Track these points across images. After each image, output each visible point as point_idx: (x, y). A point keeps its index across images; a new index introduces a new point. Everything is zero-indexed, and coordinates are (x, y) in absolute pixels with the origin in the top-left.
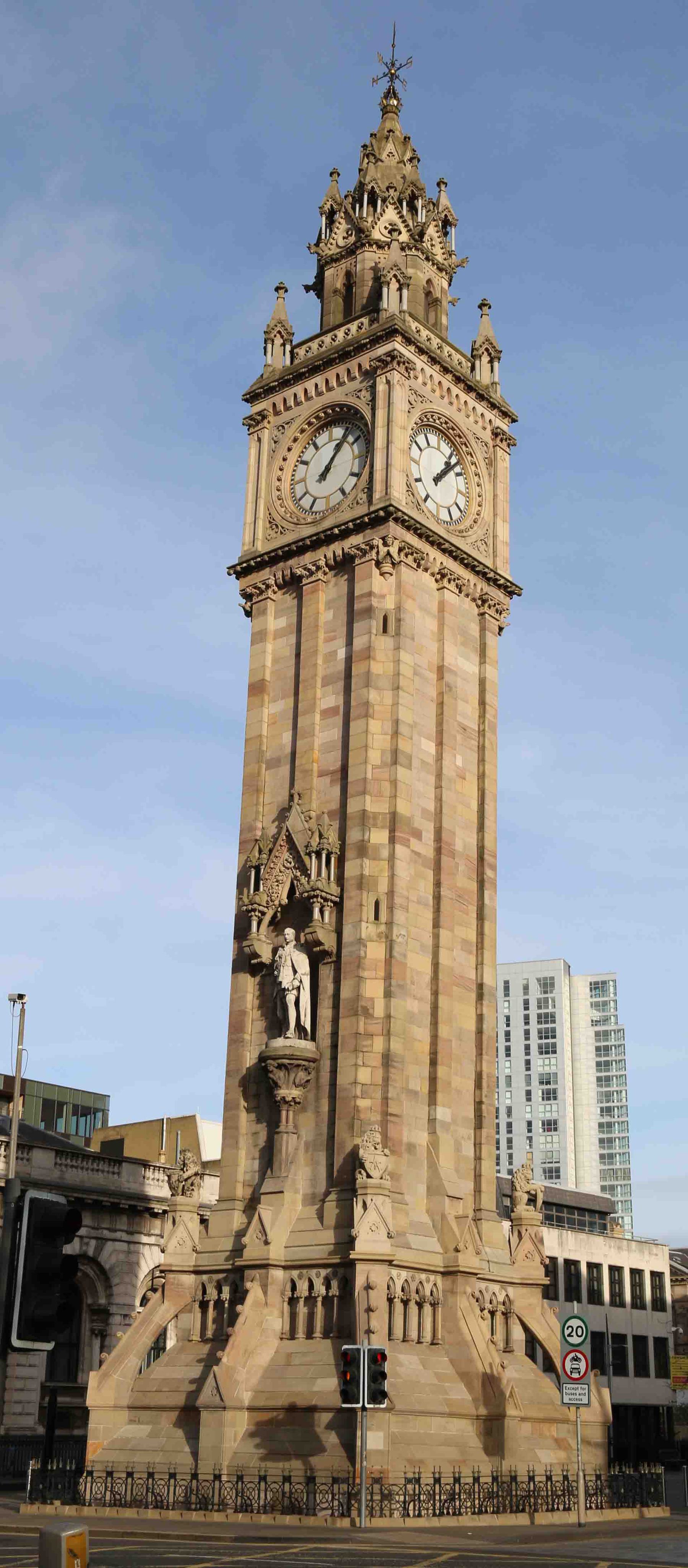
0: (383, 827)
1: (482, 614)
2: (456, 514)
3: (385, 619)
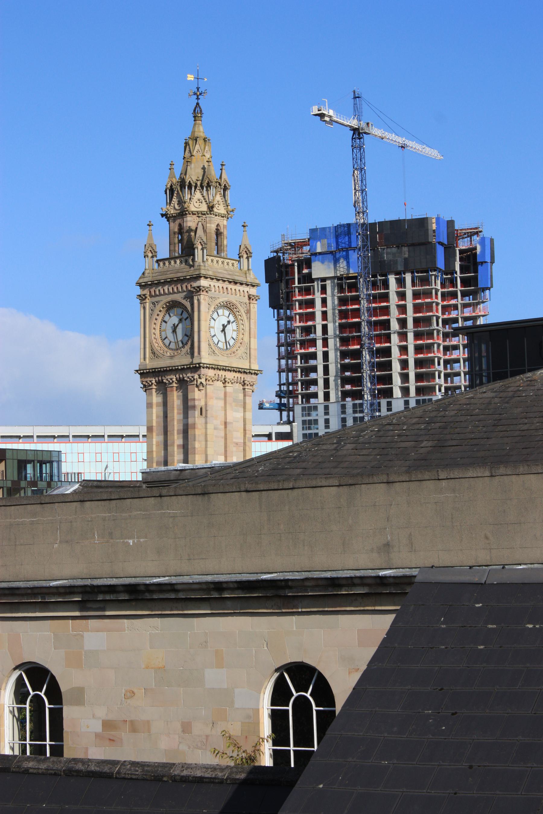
3: (201, 409)
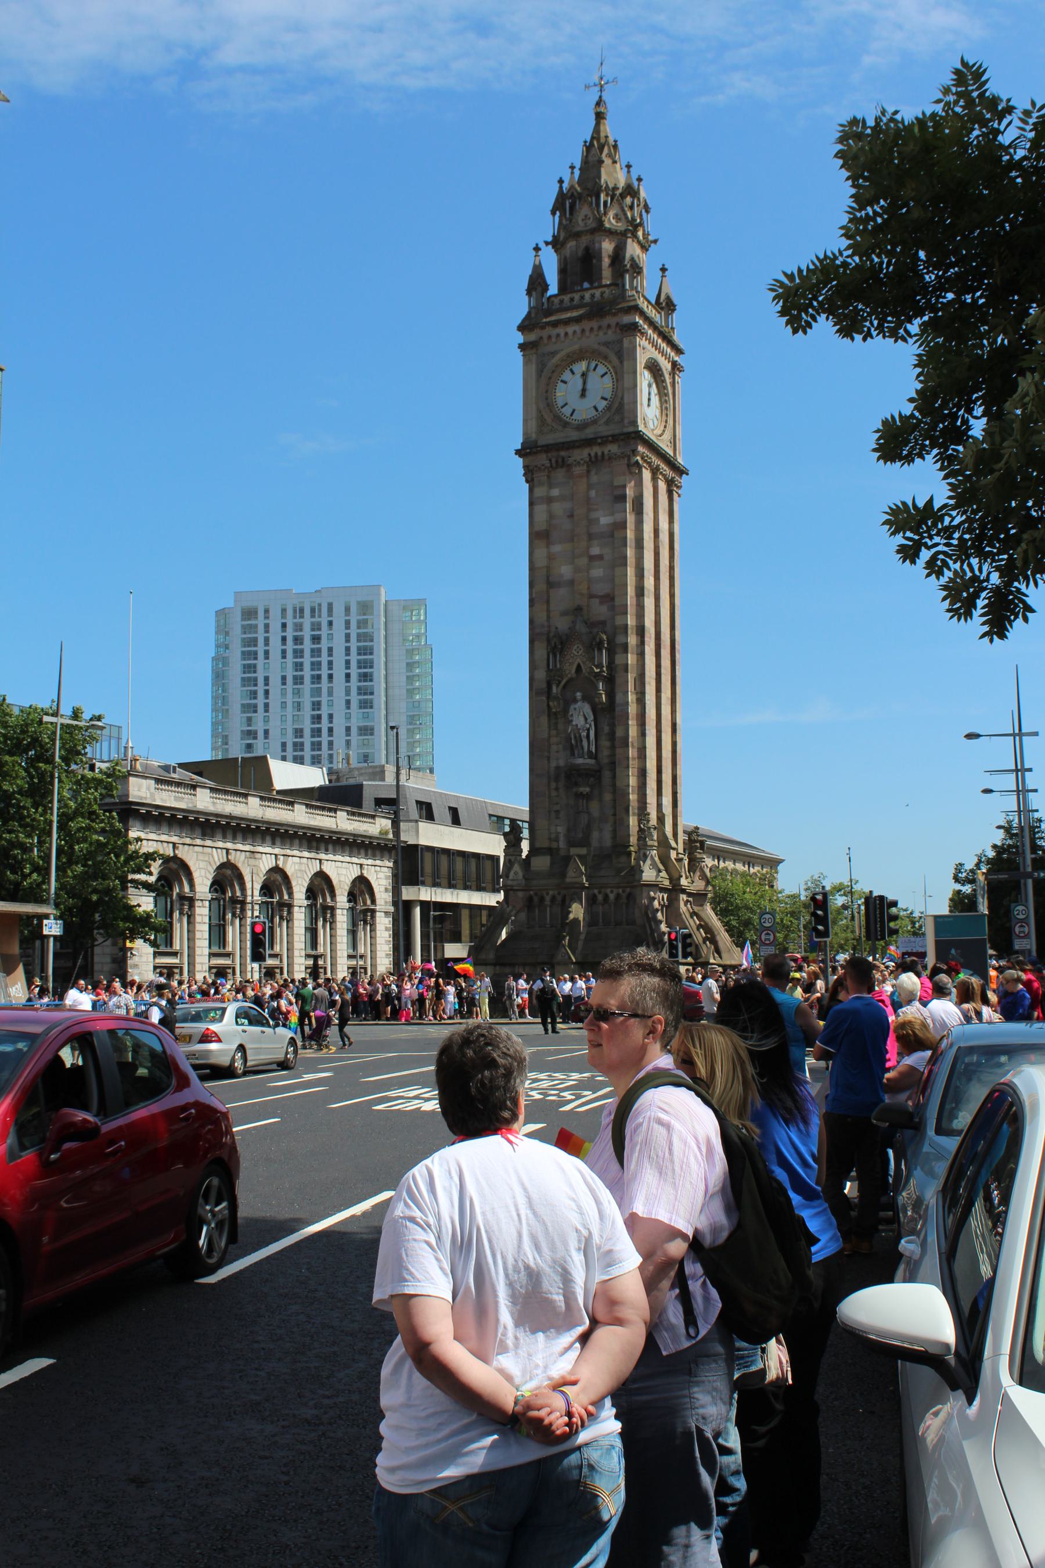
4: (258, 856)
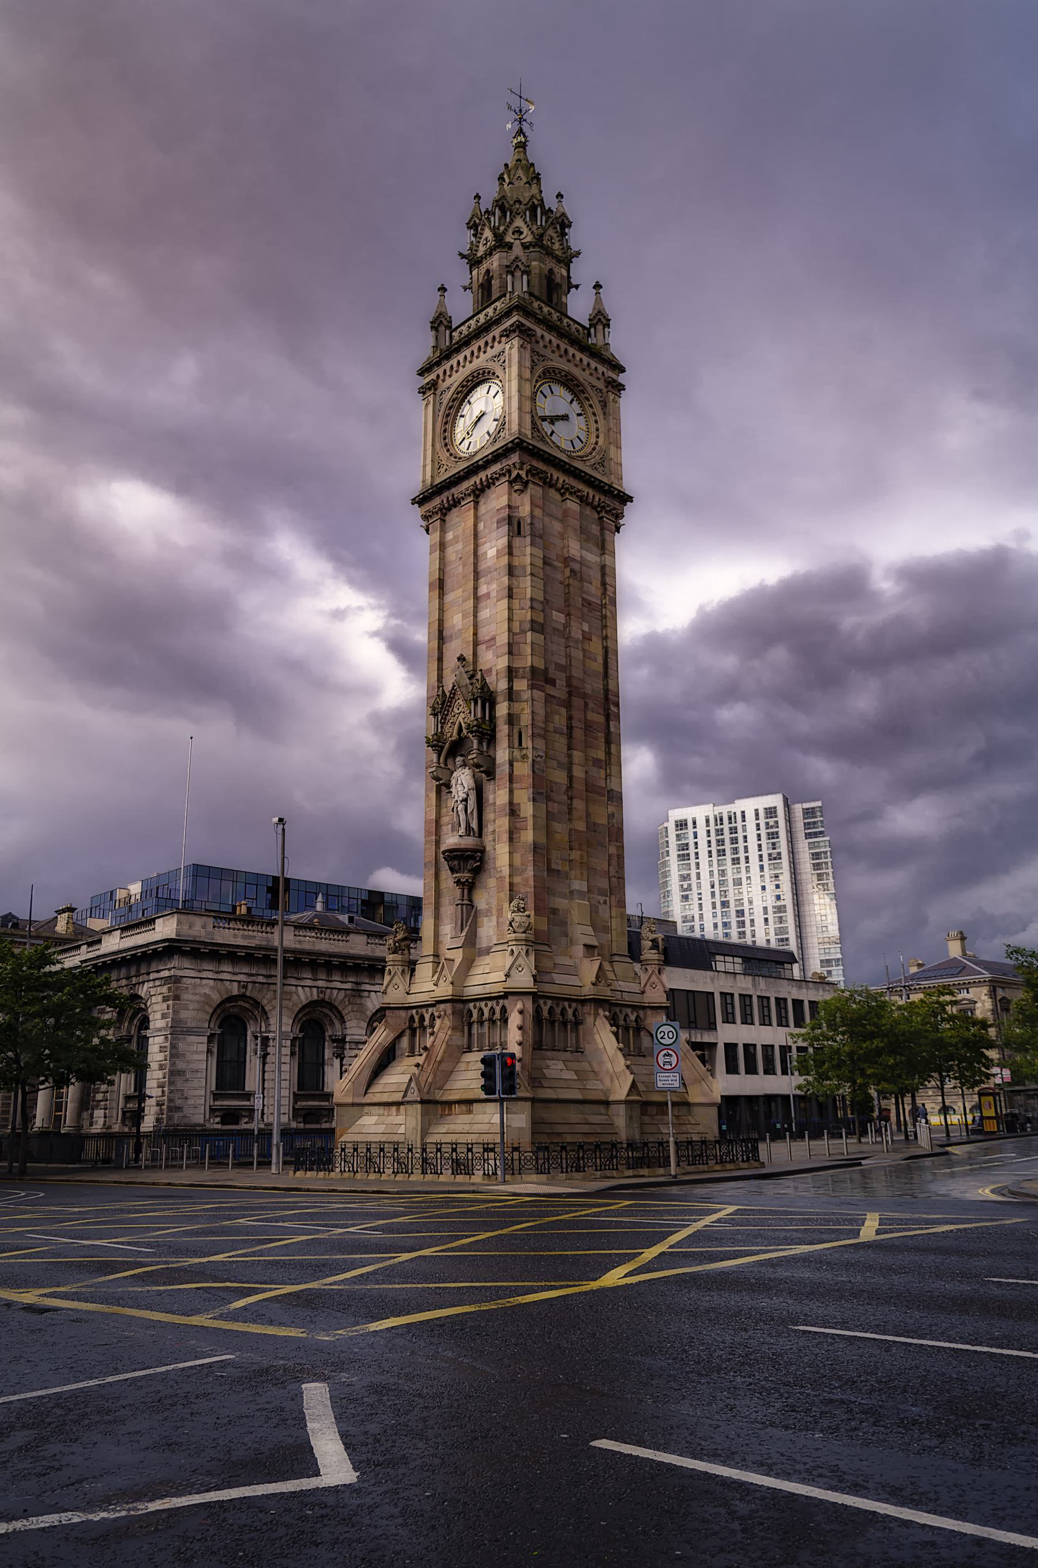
0: (523, 677)
1: (601, 518)
2: (578, 445)
4: (366, 994)
